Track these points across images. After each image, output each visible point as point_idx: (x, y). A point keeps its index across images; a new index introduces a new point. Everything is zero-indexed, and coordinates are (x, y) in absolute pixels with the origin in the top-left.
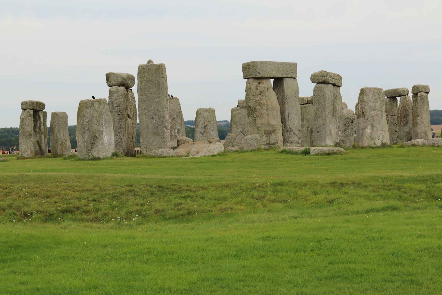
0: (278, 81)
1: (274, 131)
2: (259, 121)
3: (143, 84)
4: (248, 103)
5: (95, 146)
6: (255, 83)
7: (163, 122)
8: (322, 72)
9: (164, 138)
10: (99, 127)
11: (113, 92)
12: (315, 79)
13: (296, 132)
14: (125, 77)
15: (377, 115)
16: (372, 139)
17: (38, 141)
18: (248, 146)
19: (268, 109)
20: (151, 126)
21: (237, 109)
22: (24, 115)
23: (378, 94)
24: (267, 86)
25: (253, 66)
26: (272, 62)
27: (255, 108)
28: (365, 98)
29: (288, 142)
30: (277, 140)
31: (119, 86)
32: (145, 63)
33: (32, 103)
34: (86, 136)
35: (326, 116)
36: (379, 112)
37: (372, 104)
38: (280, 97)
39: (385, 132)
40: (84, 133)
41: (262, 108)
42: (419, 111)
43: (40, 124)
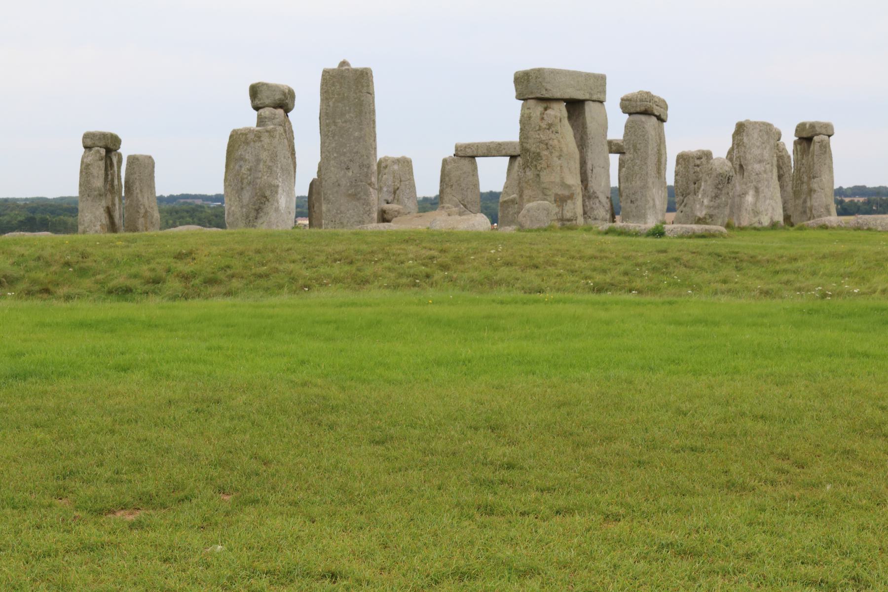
0: (575, 106)
1: (571, 197)
2: (545, 177)
3: (331, 104)
4: (525, 145)
5: (262, 214)
6: (539, 108)
7: (367, 175)
8: (641, 93)
9: (368, 204)
10: (270, 179)
15: (765, 171)
16: (756, 213)
17: (108, 208)
18: (532, 221)
19: (561, 156)
20: (344, 182)
21: (453, 160)
22: (90, 158)
23: (767, 133)
24: (559, 115)
25: (536, 77)
26: (569, 71)
27: (539, 154)
28: (745, 140)
30: (575, 213)
31: (275, 107)
32: (334, 65)
33: (104, 136)
34: (246, 196)
35: (647, 173)
36: (767, 166)
37: (756, 152)
38: (578, 136)
39: (776, 203)
40: (242, 189)
41: (551, 153)
42: (816, 167)
43: (113, 175)
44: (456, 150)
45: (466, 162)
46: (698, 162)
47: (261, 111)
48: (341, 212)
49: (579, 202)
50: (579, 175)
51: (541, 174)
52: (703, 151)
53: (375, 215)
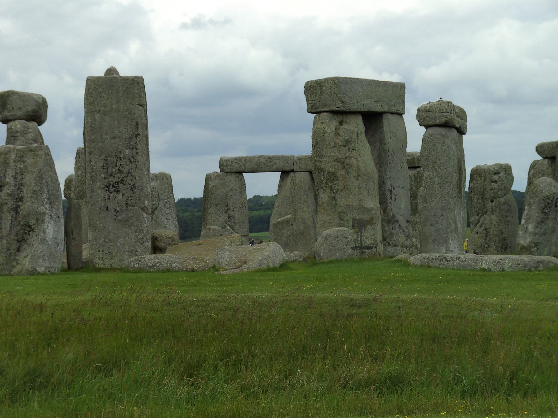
0: (372, 119)
1: (370, 222)
2: (342, 201)
4: (317, 163)
6: (334, 123)
9: (141, 231)
11: (17, 132)
12: (425, 117)
13: (404, 224)
14: (41, 101)
29: (389, 244)
30: (375, 241)
32: (102, 74)
41: (347, 173)
44: (221, 166)
45: (232, 178)
46: (496, 177)
47: (11, 124)
48: (110, 241)
49: (379, 228)
50: (378, 197)
51: (338, 196)
52: (501, 166)
53: (149, 244)
